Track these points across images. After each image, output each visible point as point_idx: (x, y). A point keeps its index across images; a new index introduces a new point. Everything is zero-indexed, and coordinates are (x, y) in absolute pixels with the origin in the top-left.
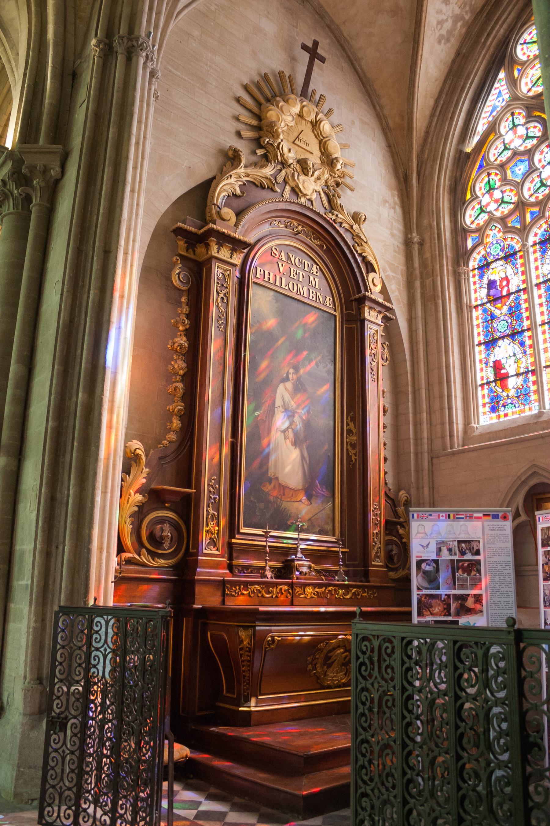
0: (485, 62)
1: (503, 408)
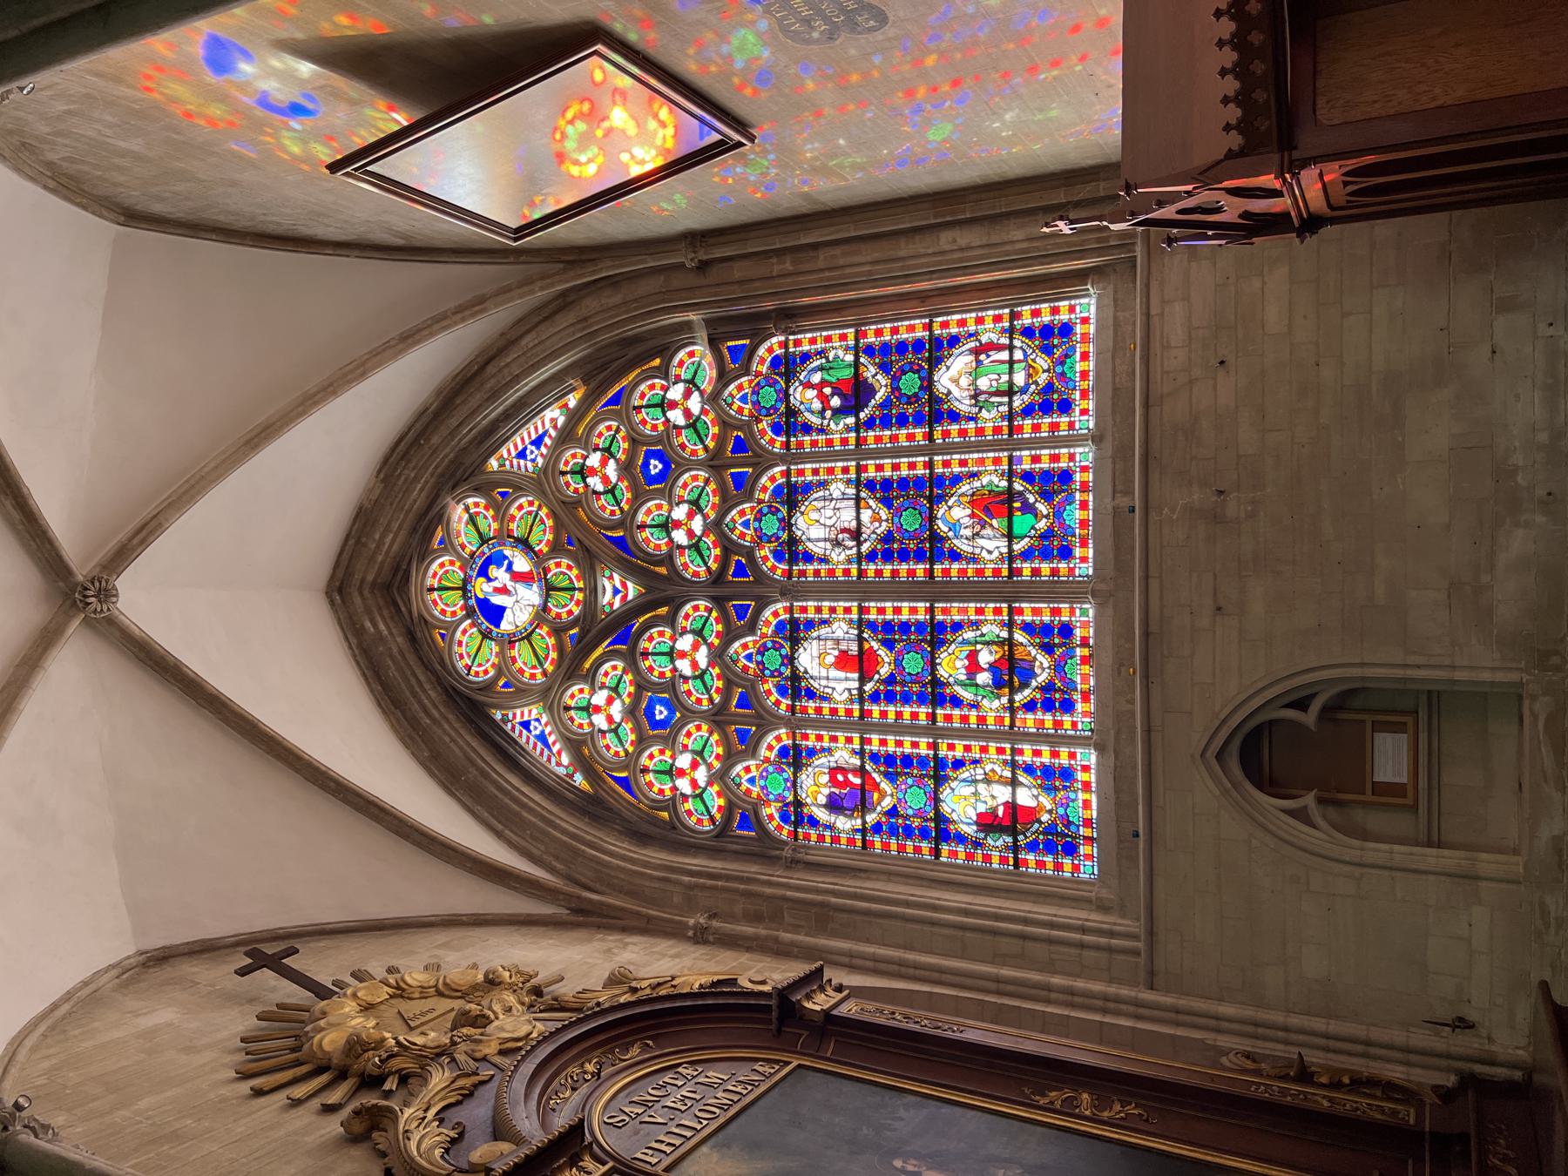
0: (462, 732)
1: (1073, 828)
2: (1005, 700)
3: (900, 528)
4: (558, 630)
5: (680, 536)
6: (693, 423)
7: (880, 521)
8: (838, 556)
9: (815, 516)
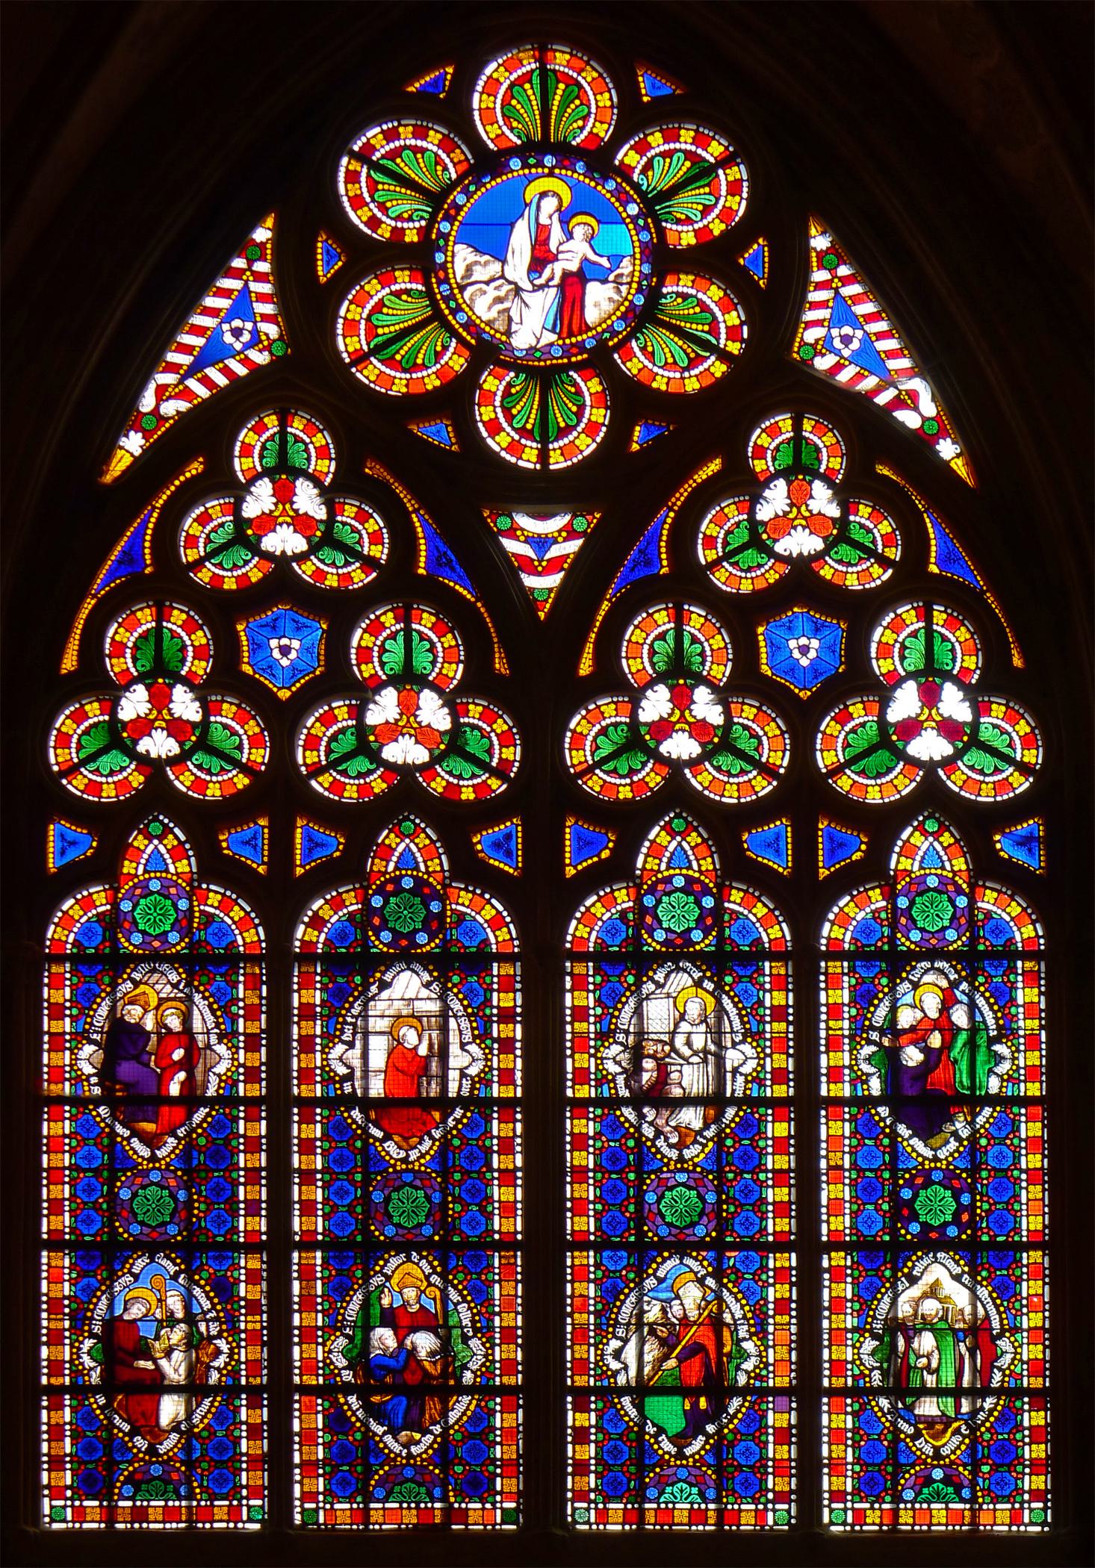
2: (348, 1376)
3: (665, 1186)
4: (456, 398)
5: (656, 704)
6: (891, 740)
7: (680, 1146)
8: (614, 1057)
9: (693, 1010)
